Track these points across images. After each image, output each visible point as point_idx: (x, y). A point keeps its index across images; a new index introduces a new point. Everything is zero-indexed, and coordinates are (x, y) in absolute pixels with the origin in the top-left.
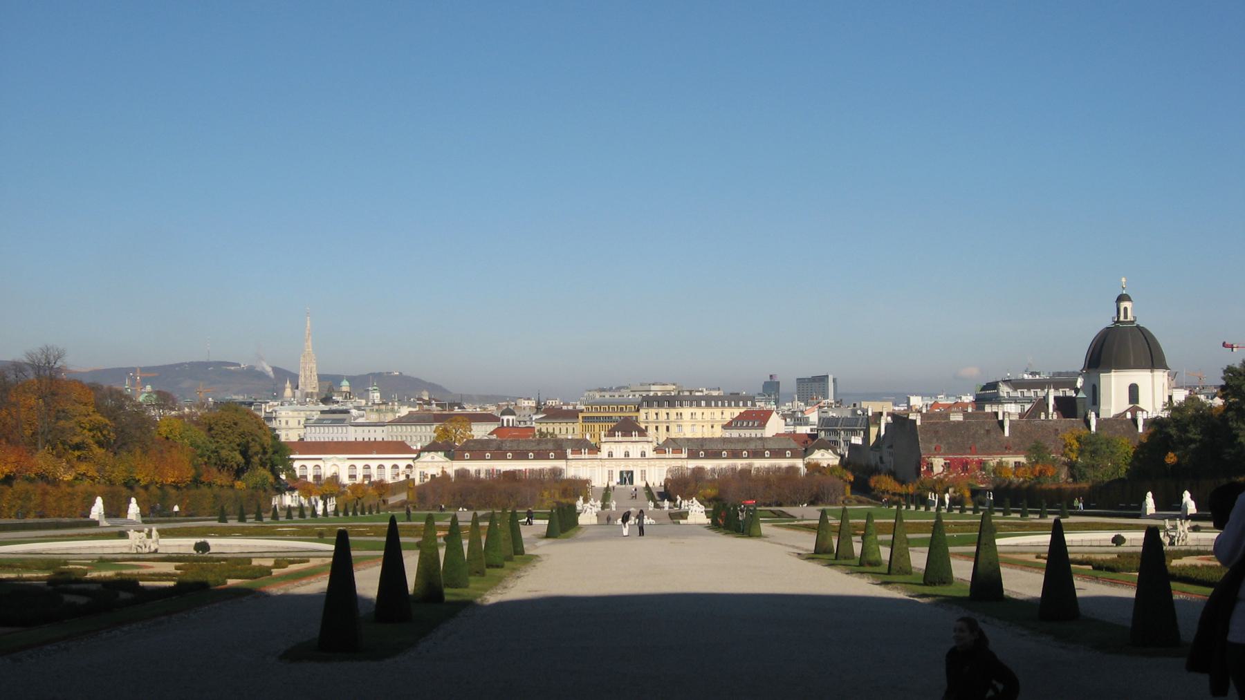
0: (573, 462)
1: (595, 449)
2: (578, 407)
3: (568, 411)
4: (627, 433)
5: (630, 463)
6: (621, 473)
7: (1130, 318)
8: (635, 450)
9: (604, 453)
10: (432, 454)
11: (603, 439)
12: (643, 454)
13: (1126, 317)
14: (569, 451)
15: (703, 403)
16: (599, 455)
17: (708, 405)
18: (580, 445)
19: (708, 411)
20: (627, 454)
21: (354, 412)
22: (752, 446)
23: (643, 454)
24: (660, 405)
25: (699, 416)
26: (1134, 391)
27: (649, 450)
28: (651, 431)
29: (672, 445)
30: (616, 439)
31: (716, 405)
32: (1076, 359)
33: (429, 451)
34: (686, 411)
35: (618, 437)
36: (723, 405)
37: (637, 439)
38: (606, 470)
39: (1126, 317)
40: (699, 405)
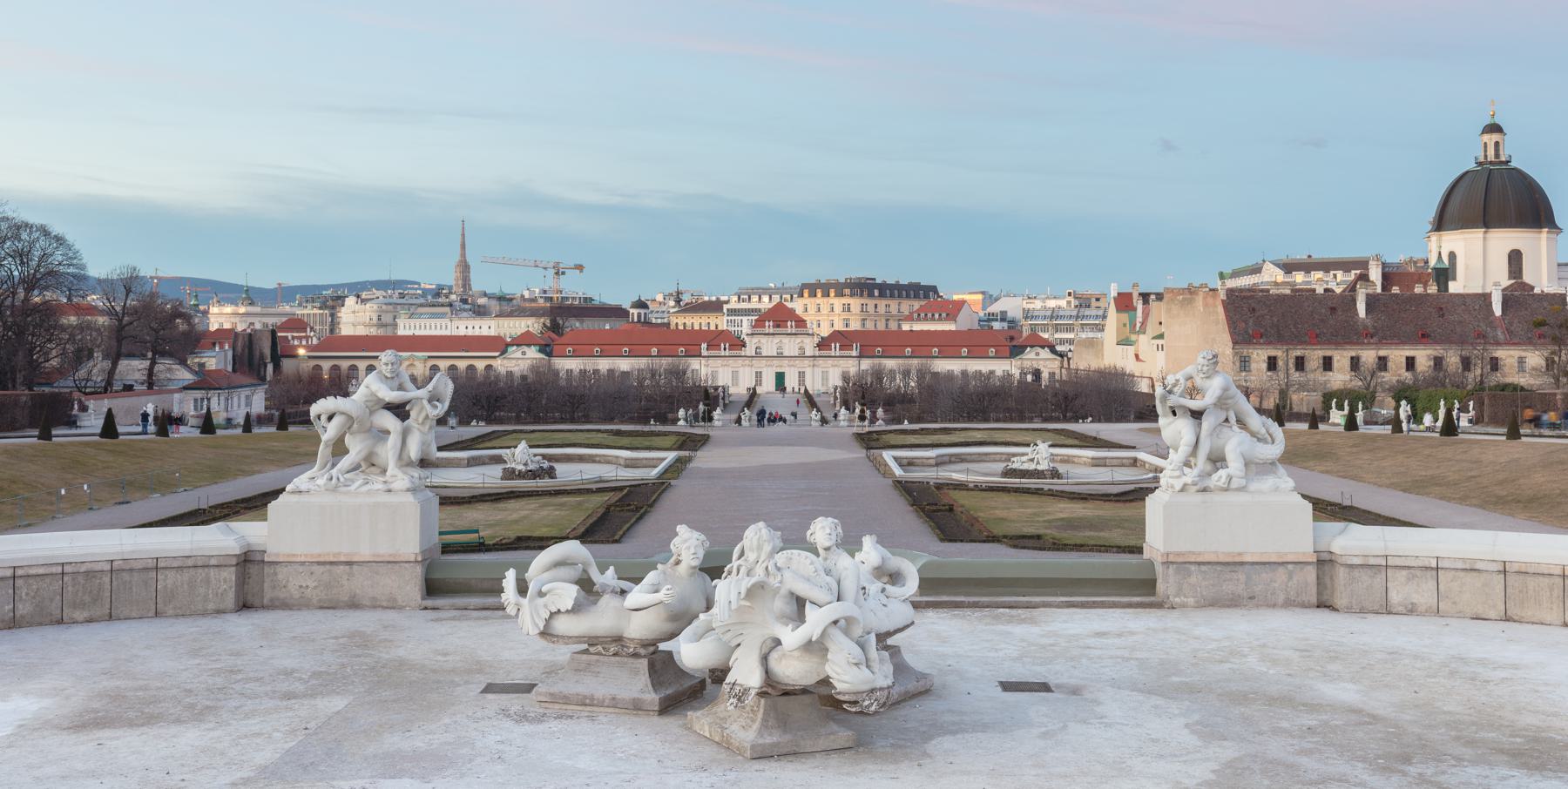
0: (711, 361)
2: (724, 298)
3: (710, 302)
8: (790, 346)
9: (750, 350)
10: (525, 348)
13: (1497, 155)
14: (704, 346)
15: (876, 293)
17: (882, 295)
19: (882, 303)
26: (1515, 258)
27: (810, 346)
29: (842, 339)
31: (892, 296)
34: (855, 303)
39: (1497, 155)
40: (871, 295)
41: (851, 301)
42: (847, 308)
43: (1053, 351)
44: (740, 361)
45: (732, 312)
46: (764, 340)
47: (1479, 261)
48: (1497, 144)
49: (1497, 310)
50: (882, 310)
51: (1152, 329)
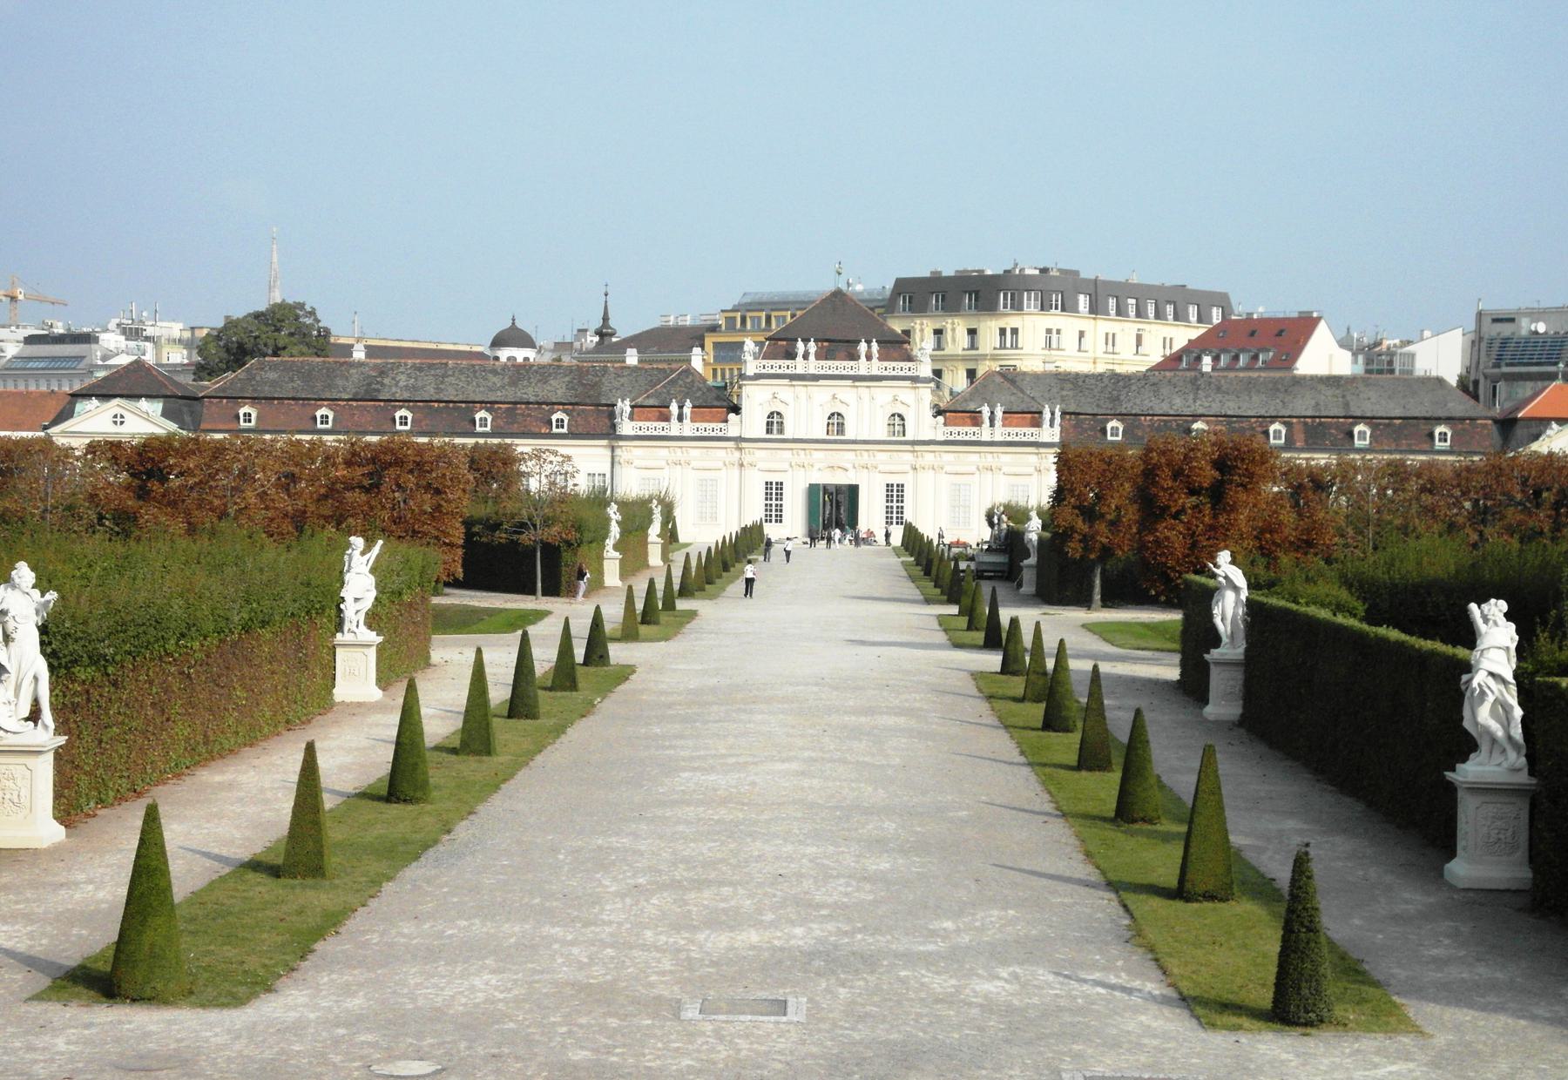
4: (838, 346)
5: (846, 457)
6: (813, 490)
9: (751, 421)
11: (752, 367)
14: (624, 406)
15: (1083, 301)
16: (734, 426)
17: (1096, 309)
19: (1098, 328)
20: (836, 422)
21: (111, 340)
22: (1303, 405)
24: (950, 306)
25: (1069, 340)
30: (799, 366)
33: (105, 397)
35: (807, 361)
36: (1140, 314)
37: (876, 367)
40: (1068, 307)
44: (722, 454)
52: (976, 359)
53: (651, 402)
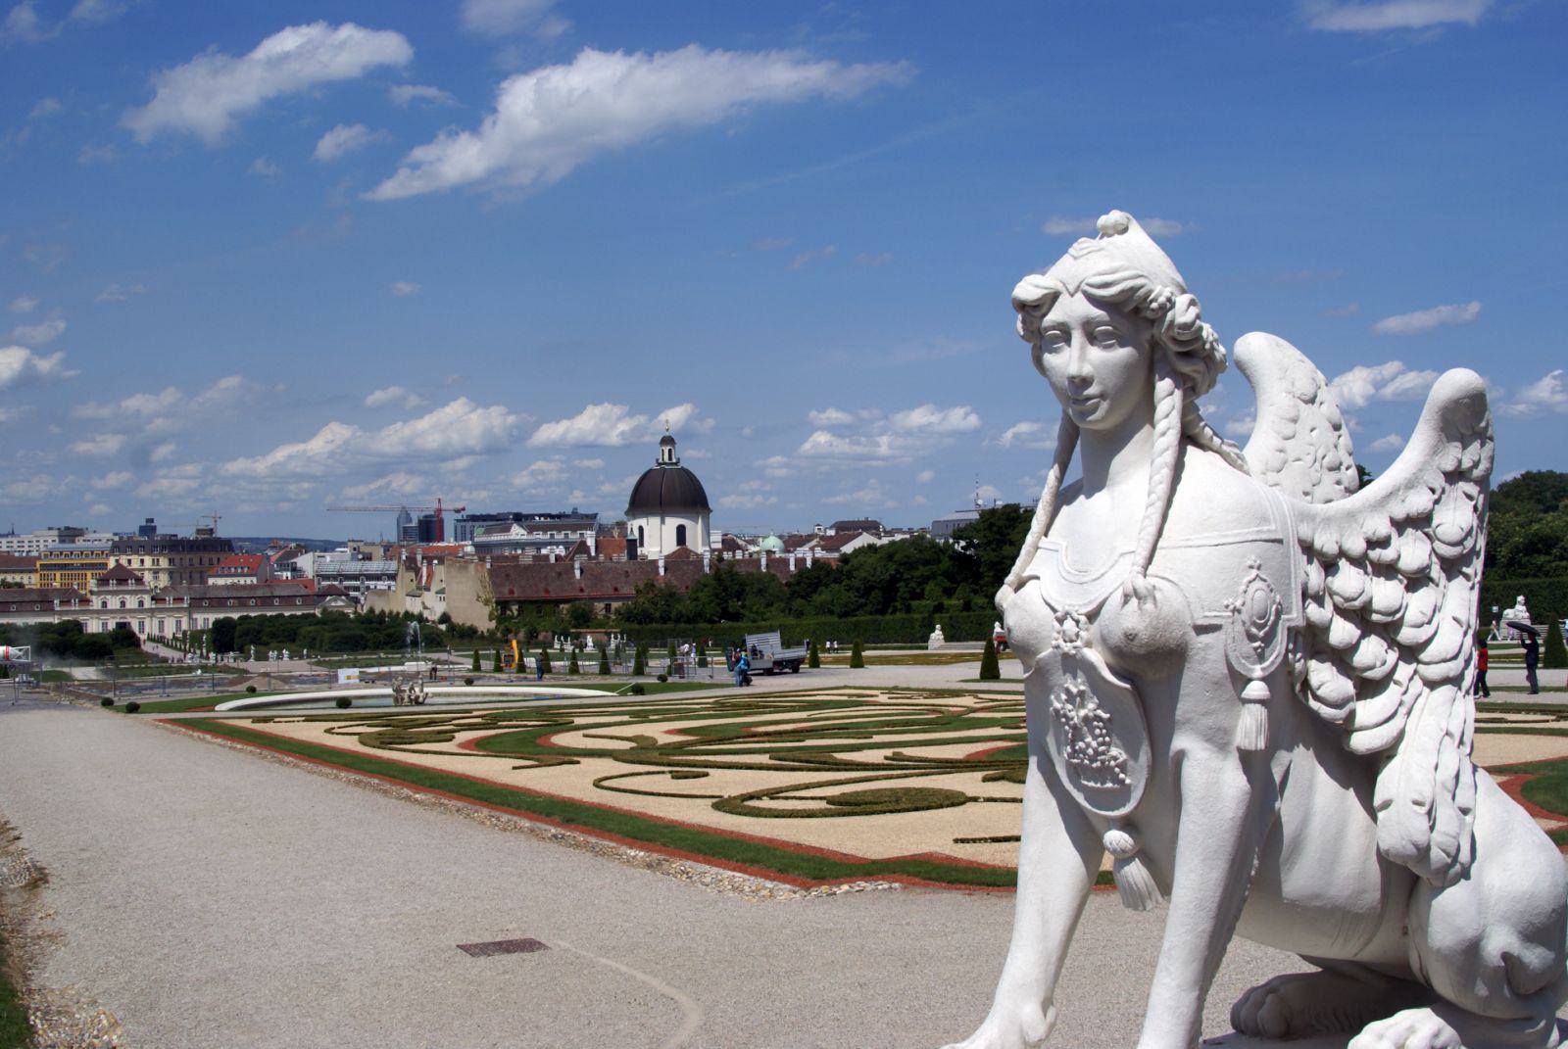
1: (85, 601)
4: (122, 581)
7: (674, 461)
8: (132, 602)
9: (96, 603)
12: (141, 603)
18: (67, 596)
20: (123, 604)
22: (260, 593)
23: (141, 603)
25: (177, 561)
26: (681, 530)
27: (147, 599)
28: (148, 577)
32: (610, 500)
35: (112, 586)
38: (101, 622)
39: (670, 459)
40: (178, 551)
41: (161, 559)
42: (156, 562)
43: (347, 595)
45: (44, 567)
46: (109, 597)
47: (658, 538)
48: (670, 451)
49: (662, 572)
50: (186, 562)
51: (434, 588)
52: (144, 570)
53: (65, 600)
